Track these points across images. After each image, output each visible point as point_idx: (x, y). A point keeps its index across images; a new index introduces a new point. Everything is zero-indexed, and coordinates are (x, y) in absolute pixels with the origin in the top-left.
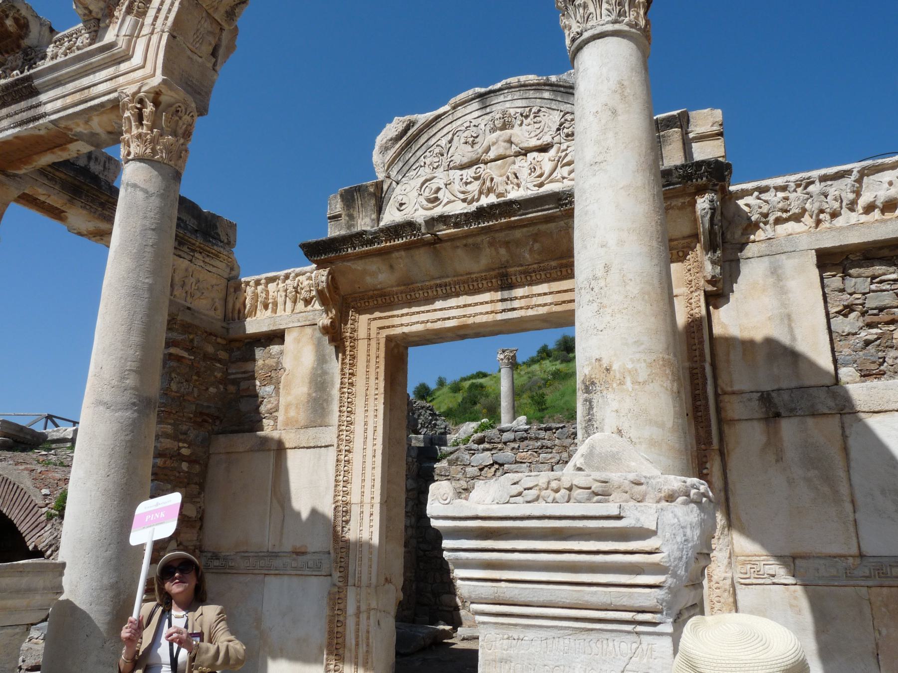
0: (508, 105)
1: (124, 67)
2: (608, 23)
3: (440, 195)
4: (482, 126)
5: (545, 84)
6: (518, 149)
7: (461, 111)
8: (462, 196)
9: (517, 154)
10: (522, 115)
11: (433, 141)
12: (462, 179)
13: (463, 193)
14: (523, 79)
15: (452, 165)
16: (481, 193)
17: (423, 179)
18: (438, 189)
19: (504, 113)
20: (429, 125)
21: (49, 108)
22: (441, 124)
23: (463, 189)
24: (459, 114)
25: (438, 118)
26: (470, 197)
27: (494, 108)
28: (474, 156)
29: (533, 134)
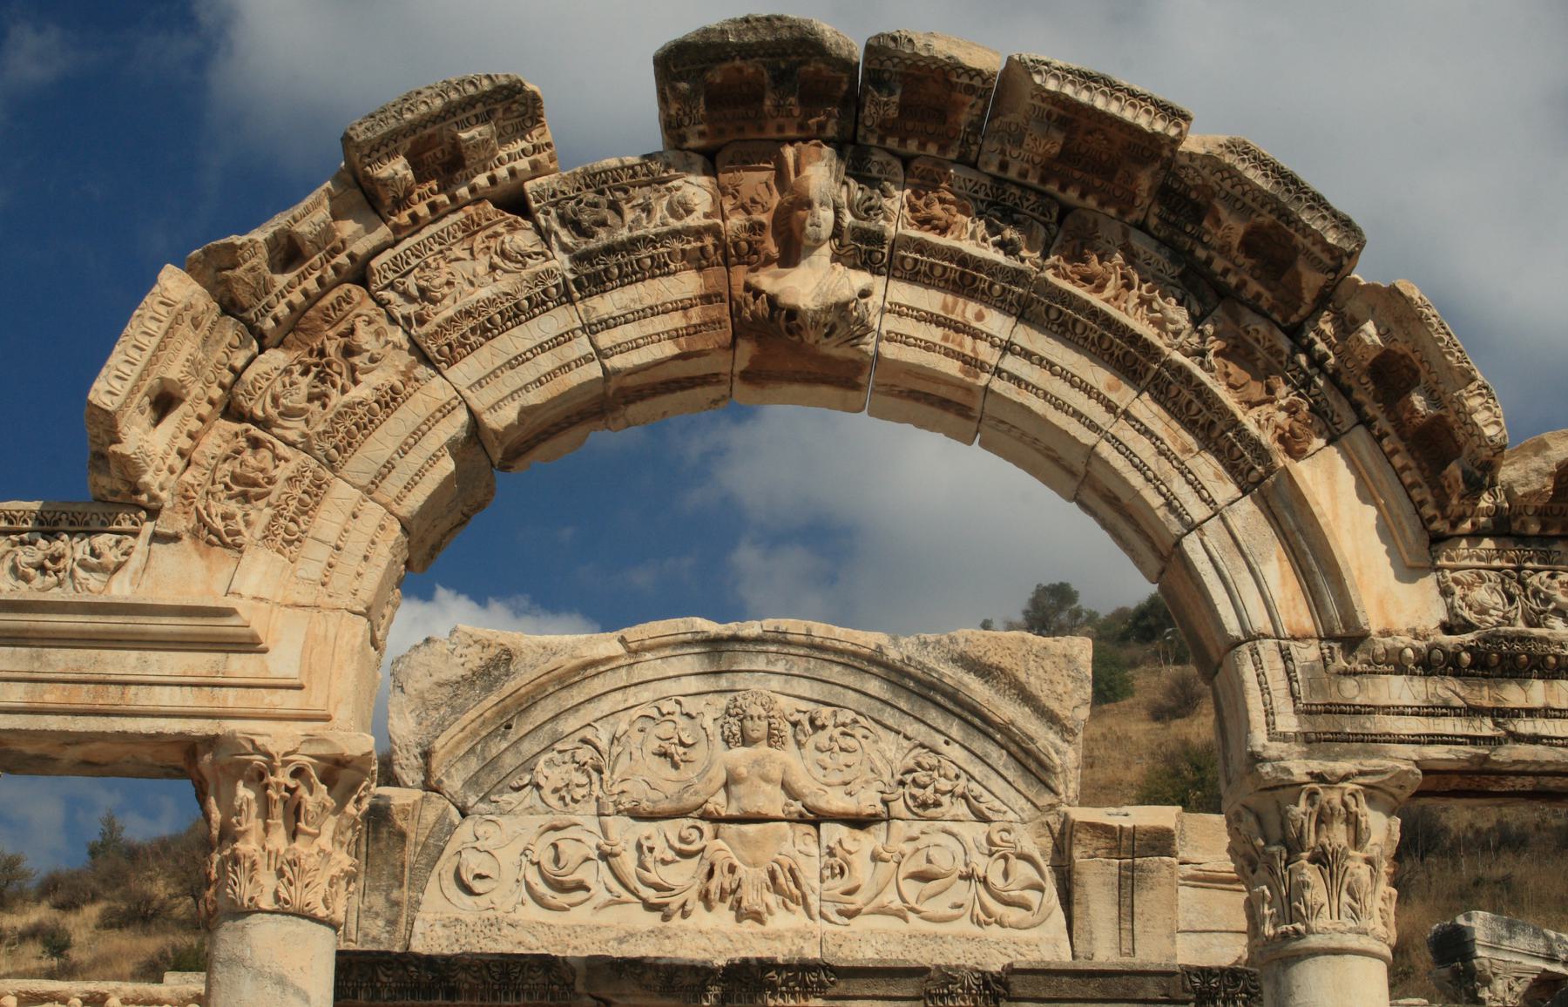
0: (776, 683)
1: (240, 666)
2: (1350, 930)
3: (586, 874)
5: (871, 660)
6: (798, 806)
7: (650, 666)
8: (651, 895)
9: (802, 820)
10: (812, 721)
11: (569, 724)
12: (651, 850)
13: (658, 887)
14: (820, 630)
17: (547, 820)
18: (588, 859)
19: (769, 706)
20: (565, 680)
22: (597, 686)
23: (652, 877)
24: (645, 671)
25: (590, 667)
27: (741, 682)
28: (690, 800)
29: (836, 778)
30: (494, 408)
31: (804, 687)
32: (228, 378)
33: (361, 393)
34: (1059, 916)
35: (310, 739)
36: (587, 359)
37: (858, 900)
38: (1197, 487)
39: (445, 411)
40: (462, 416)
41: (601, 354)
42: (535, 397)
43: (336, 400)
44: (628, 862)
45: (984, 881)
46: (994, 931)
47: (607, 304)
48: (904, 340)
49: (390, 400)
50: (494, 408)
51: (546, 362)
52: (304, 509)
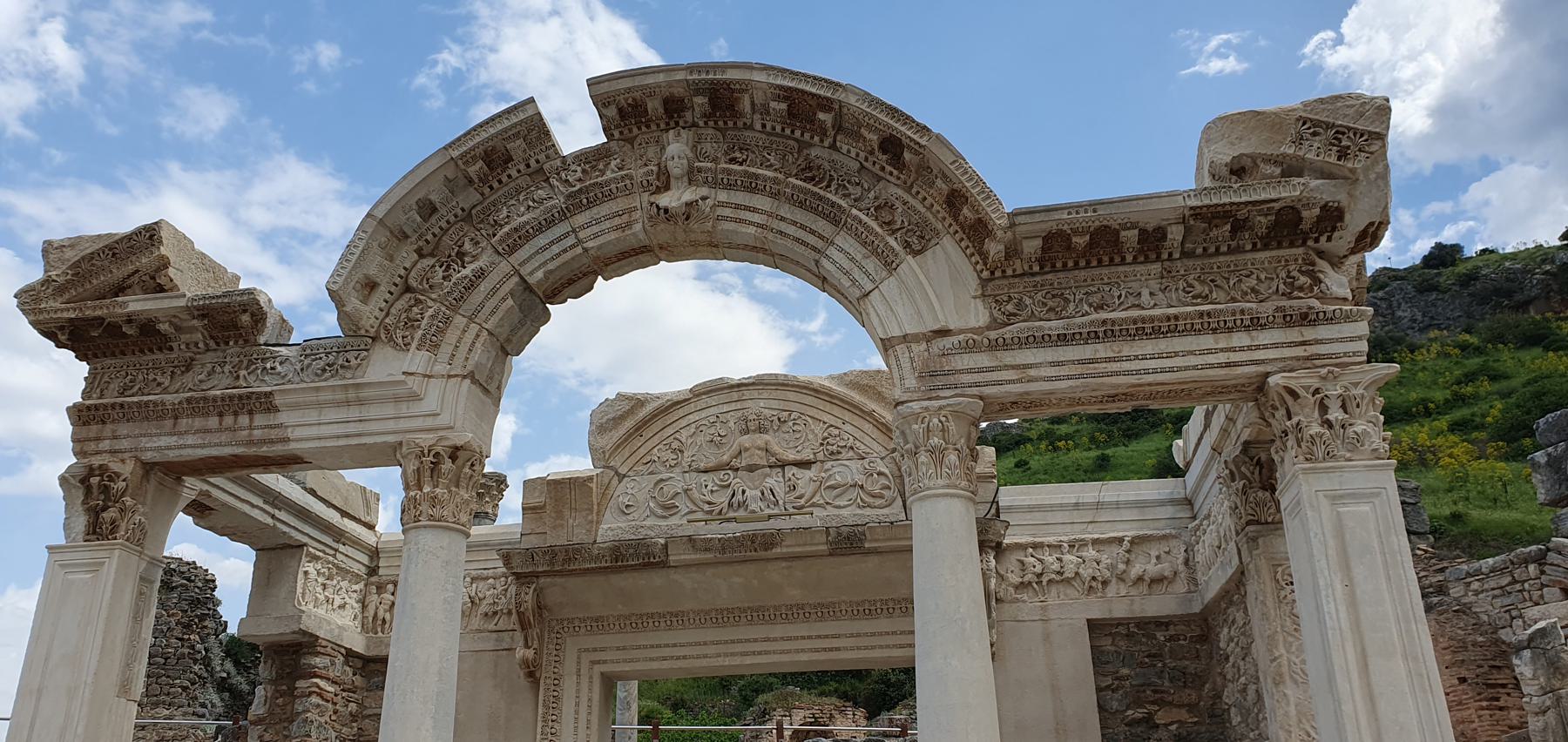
4: (731, 424)
11: (670, 431)
13: (709, 503)
15: (694, 465)
16: (730, 505)
21: (299, 433)
22: (681, 413)
26: (717, 509)
30: (531, 273)
31: (774, 404)
32: (403, 272)
33: (467, 272)
34: (899, 502)
35: (441, 439)
36: (572, 247)
37: (802, 501)
38: (868, 275)
39: (508, 277)
40: (516, 279)
41: (580, 242)
42: (550, 266)
43: (455, 277)
44: (696, 494)
45: (862, 487)
46: (868, 511)
47: (580, 219)
48: (725, 218)
49: (481, 274)
50: (531, 273)
51: (556, 249)
52: (441, 331)
